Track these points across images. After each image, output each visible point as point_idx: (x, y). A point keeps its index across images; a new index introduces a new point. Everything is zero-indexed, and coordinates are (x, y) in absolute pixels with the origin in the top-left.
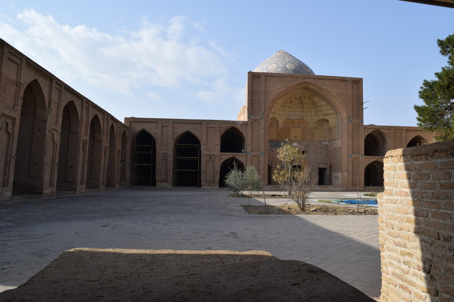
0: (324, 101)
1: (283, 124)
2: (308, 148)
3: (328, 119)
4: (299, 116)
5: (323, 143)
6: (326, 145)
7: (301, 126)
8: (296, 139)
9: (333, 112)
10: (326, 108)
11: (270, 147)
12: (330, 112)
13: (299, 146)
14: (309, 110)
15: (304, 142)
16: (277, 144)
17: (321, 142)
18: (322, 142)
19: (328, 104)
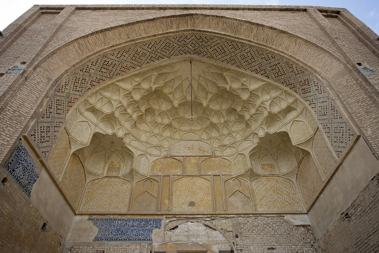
0: (254, 74)
1: (153, 169)
2: (238, 239)
3: (283, 130)
4: (202, 148)
5: (292, 220)
6: (303, 226)
7: (209, 173)
8: (193, 210)
9: (291, 100)
10: (266, 97)
11: (96, 239)
12: (284, 105)
13: (204, 232)
14: (225, 132)
15: (224, 221)
16: (126, 227)
17: (280, 215)
18: (286, 217)
19: (268, 77)
